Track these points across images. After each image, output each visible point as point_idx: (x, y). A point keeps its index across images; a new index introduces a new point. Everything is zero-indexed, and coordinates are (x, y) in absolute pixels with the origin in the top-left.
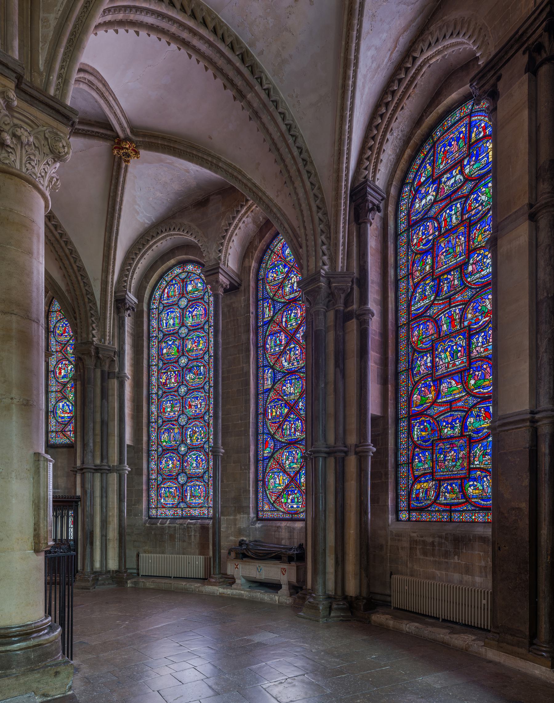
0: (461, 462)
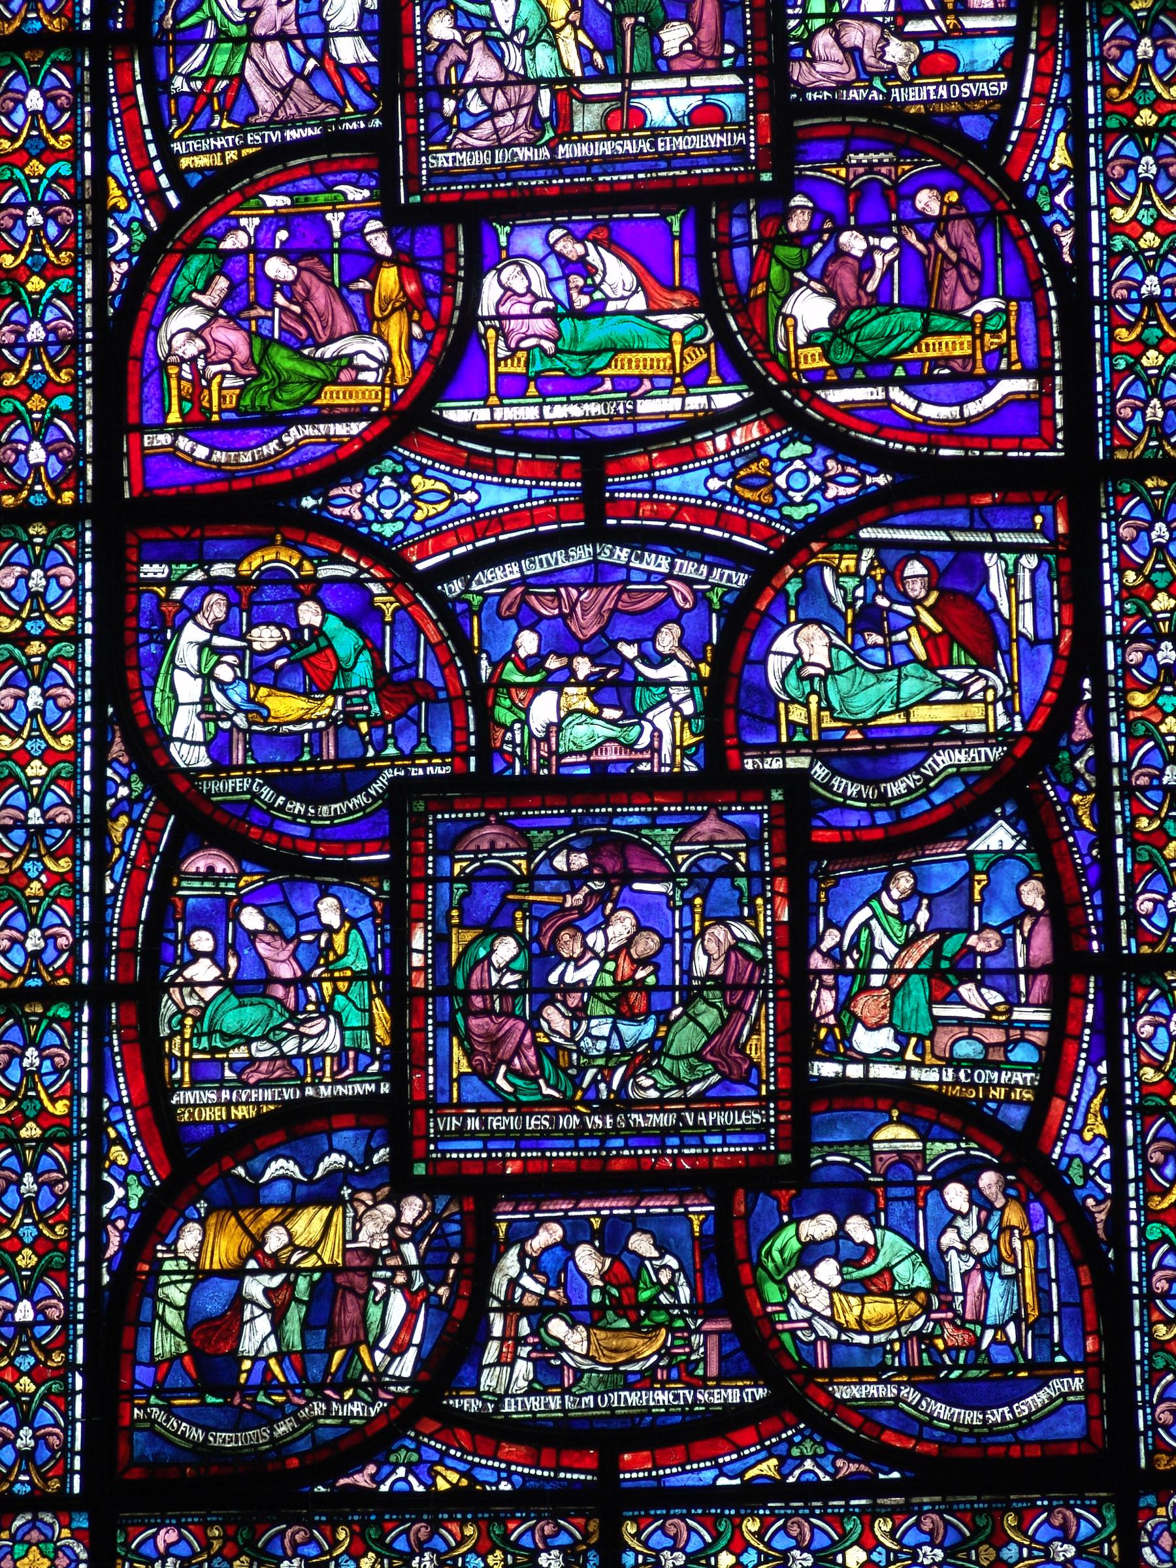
0: (710, 1018)
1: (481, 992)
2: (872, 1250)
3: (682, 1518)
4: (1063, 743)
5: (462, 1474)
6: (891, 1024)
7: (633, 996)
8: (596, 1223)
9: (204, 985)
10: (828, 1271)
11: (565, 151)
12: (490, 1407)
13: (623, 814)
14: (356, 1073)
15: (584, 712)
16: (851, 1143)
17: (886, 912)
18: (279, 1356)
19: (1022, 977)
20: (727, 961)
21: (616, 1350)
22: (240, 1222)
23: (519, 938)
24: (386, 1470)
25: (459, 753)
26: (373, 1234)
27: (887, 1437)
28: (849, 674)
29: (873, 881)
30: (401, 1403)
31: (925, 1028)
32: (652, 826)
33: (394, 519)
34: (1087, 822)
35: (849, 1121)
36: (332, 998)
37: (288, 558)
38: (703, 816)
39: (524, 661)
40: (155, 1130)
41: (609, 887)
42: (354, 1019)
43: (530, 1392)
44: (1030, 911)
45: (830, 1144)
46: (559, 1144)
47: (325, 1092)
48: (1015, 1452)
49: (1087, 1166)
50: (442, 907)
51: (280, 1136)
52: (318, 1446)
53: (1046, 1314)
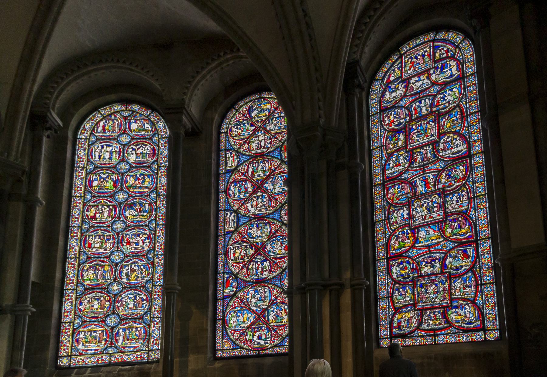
0: (442, 293)
11: (425, 221)
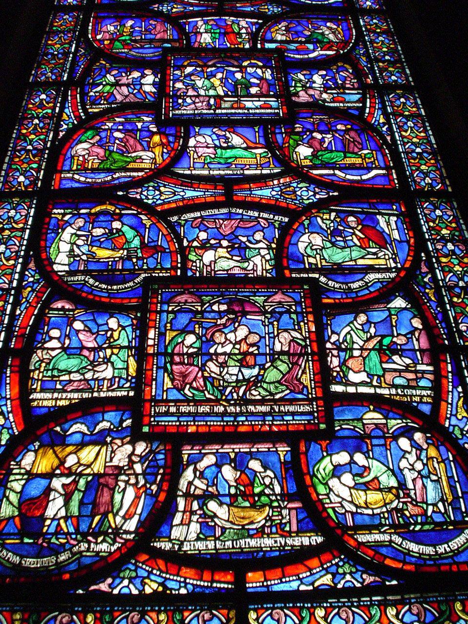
0: (283, 367)
1: (179, 354)
2: (367, 469)
3: (282, 609)
4: (418, 273)
5: (160, 584)
6: (364, 371)
7: (248, 358)
8: (232, 456)
9: (53, 349)
10: (347, 478)
11: (218, 111)
12: (176, 547)
13: (242, 292)
14: (119, 387)
15: (226, 257)
16: (353, 420)
17: (357, 328)
18: (66, 518)
19: (418, 353)
20: (290, 345)
21: (243, 518)
22: (55, 452)
23: (197, 335)
24: (118, 581)
25: (174, 268)
26: (120, 458)
27: (388, 562)
28: (331, 249)
29: (350, 317)
30: (128, 544)
31: (381, 373)
32: (255, 296)
33: (153, 199)
34: (433, 299)
35: (350, 410)
36: (110, 356)
37: (111, 208)
38: (276, 293)
39: (201, 241)
40: (19, 410)
41: (237, 317)
42: (120, 365)
43: (198, 539)
44: (416, 329)
45: (343, 420)
46: (214, 419)
47: (103, 395)
48: (455, 568)
49: (462, 430)
50: (163, 323)
51: (79, 414)
52: (81, 567)
53: (456, 498)
